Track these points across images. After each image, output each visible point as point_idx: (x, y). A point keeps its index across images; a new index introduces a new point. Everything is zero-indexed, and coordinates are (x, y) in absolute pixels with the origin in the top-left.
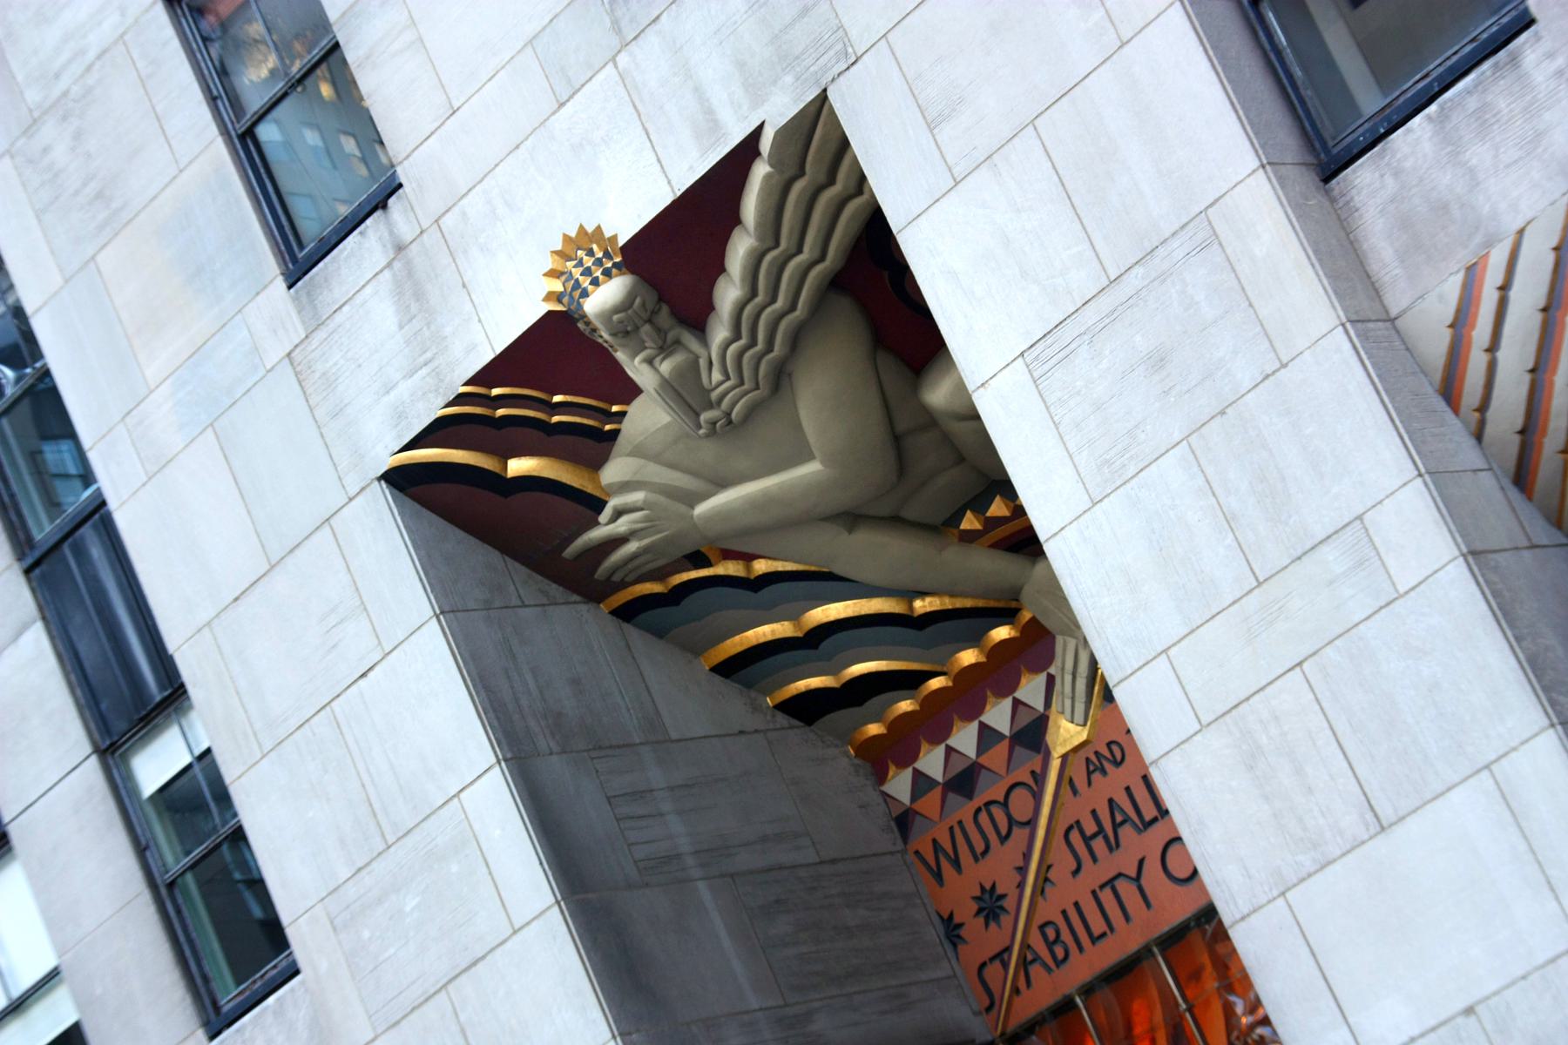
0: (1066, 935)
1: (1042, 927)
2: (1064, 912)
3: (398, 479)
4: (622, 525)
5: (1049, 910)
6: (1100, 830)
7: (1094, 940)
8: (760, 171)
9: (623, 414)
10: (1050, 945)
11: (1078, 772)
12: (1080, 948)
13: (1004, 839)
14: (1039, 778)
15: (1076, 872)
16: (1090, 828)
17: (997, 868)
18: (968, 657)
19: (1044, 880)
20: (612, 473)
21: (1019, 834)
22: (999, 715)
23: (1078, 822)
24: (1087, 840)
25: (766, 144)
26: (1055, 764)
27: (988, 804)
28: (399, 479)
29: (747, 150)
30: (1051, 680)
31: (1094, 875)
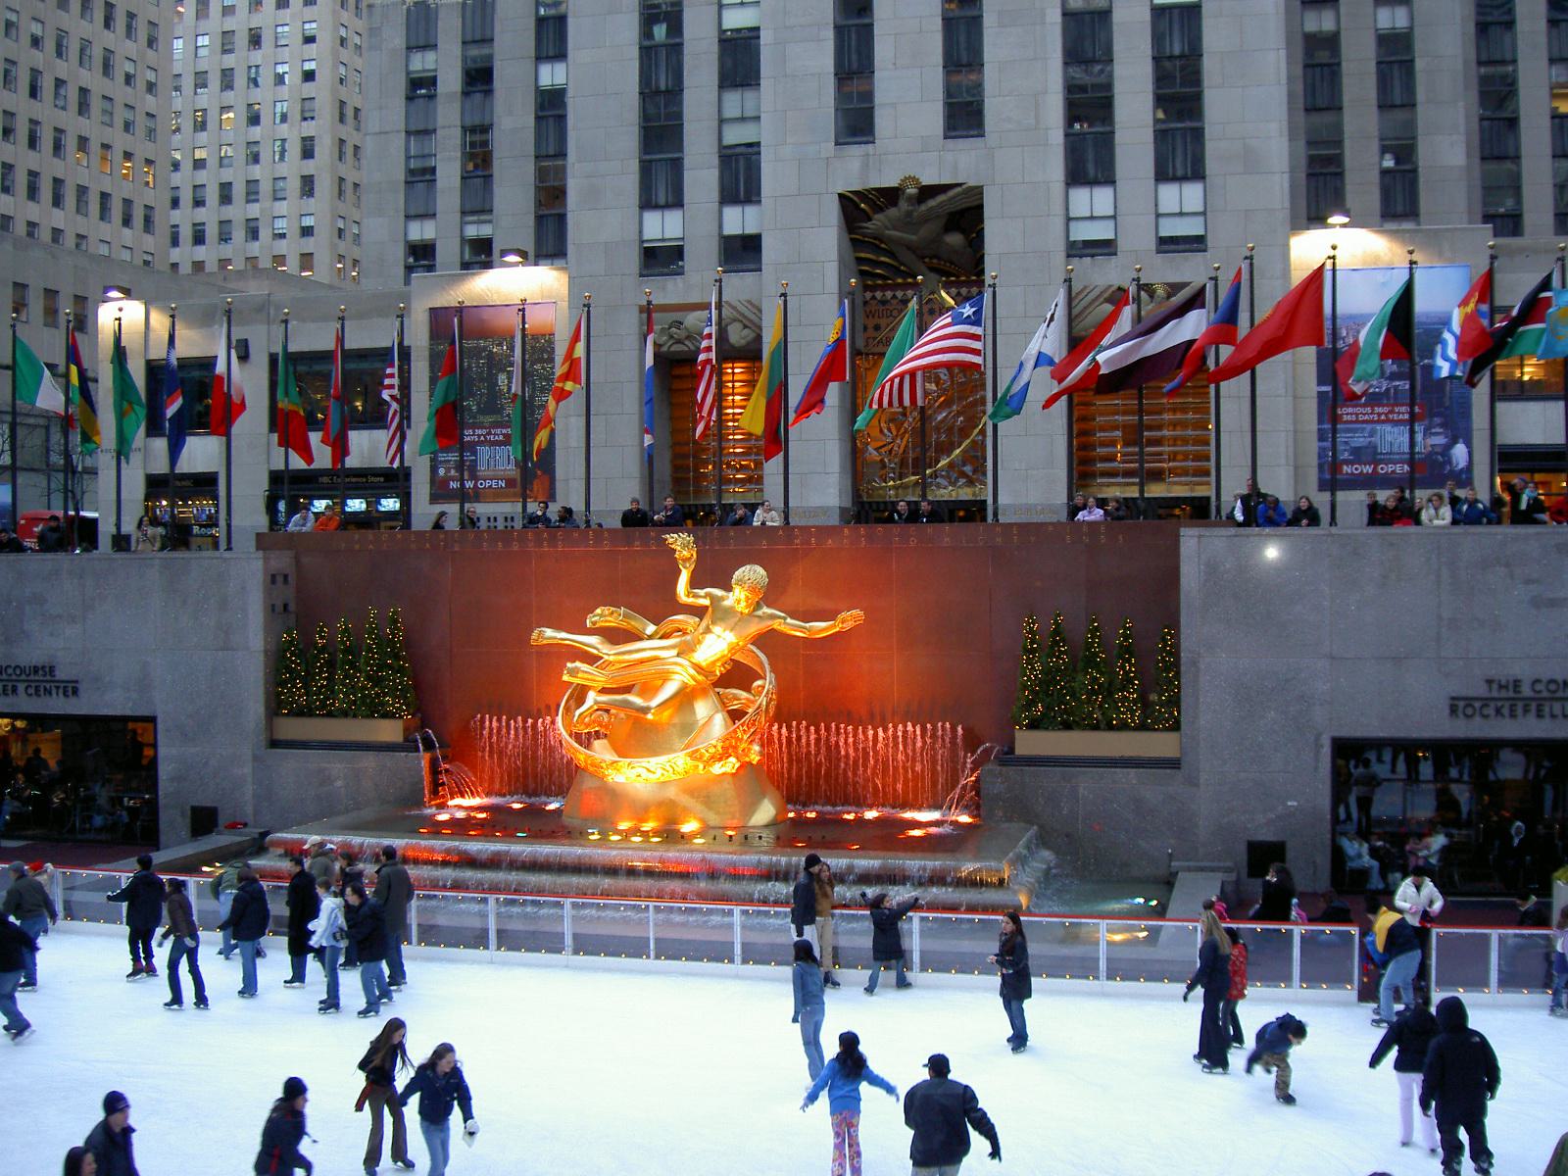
3: (841, 196)
8: (959, 189)
17: (883, 322)
18: (900, 281)
20: (876, 216)
22: (899, 294)
25: (964, 187)
28: (841, 196)
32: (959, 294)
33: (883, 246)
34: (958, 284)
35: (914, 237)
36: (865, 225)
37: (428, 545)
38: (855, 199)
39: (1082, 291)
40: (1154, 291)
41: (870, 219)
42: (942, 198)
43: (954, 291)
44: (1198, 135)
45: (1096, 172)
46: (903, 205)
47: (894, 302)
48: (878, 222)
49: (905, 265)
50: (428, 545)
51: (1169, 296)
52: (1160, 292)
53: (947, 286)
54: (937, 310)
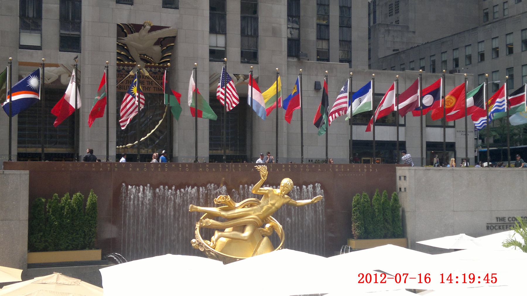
0: (122, 87)
1: (120, 86)
2: (123, 86)
3: (118, 25)
4: (125, 39)
5: (122, 85)
6: (130, 82)
7: (124, 89)
8: (167, 29)
9: (135, 33)
10: (120, 87)
11: (131, 77)
12: (123, 89)
13: (120, 77)
14: (127, 75)
15: (126, 84)
16: (129, 81)
18: (126, 63)
19: (122, 82)
21: (122, 78)
22: (126, 68)
23: (128, 80)
24: (128, 82)
25: (169, 28)
26: (129, 75)
27: (120, 74)
29: (168, 27)
30: (132, 69)
31: (127, 85)
32: (151, 71)
33: (125, 47)
34: (151, 67)
35: (141, 46)
36: (123, 38)
37: (101, 169)
38: (122, 26)
39: (213, 75)
40: (239, 78)
41: (126, 36)
42: (159, 32)
43: (149, 69)
44: (256, 19)
45: (219, 29)
46: (143, 32)
47: (124, 71)
48: (130, 39)
49: (131, 57)
50: (101, 169)
51: (245, 79)
52: (242, 78)
53: (146, 67)
54: (142, 76)
